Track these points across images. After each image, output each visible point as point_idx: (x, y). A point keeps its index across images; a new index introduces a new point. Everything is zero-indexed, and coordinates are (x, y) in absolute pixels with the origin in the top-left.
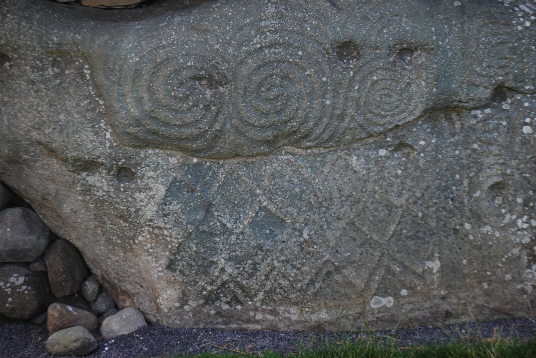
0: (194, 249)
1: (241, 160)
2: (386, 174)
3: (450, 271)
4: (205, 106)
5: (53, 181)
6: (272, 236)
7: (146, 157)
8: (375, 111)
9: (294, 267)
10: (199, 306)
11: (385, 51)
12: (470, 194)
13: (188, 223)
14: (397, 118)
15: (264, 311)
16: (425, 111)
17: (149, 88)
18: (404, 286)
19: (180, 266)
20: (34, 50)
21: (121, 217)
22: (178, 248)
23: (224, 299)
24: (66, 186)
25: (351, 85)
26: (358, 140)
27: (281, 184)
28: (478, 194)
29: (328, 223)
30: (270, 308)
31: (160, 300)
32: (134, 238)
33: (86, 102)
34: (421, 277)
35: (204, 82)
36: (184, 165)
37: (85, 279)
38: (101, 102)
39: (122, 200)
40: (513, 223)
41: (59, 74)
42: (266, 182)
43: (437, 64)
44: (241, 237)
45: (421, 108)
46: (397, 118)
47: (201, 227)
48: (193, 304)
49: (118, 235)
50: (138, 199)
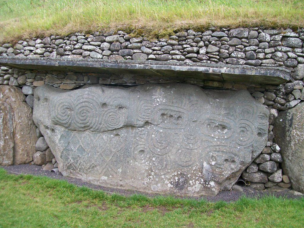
3: (124, 173)
6: (82, 154)
25: (103, 115)
34: (116, 173)
35: (69, 110)
42: (82, 139)
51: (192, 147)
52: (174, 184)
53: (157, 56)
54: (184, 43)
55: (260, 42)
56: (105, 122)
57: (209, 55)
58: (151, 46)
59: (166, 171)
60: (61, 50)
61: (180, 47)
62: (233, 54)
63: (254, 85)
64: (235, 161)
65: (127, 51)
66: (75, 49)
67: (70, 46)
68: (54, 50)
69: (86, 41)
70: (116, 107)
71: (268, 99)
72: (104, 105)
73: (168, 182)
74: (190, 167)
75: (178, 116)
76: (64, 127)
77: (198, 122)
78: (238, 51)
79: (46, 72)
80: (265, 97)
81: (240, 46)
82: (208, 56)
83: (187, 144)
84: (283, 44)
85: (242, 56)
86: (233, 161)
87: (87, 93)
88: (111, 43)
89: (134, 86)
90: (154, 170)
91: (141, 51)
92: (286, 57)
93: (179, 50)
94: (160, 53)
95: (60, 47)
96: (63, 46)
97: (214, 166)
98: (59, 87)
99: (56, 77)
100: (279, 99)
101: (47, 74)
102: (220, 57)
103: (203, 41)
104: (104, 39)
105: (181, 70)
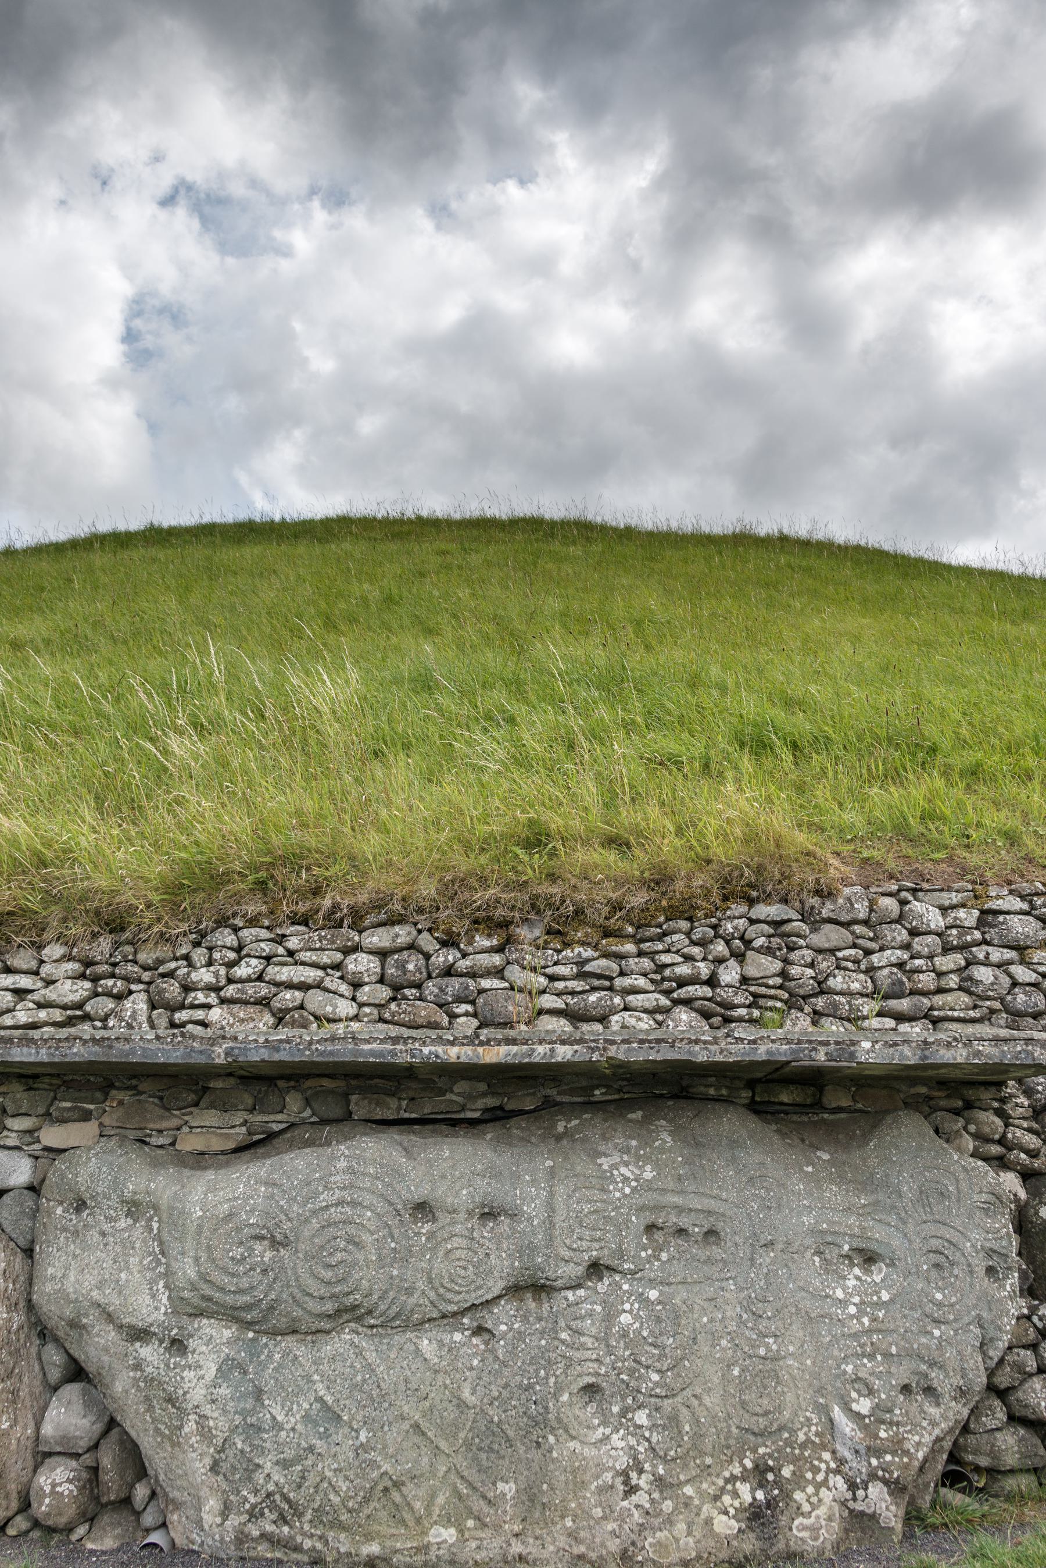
0: (240, 1446)
1: (299, 1336)
6: (326, 1436)
9: (346, 1478)
11: (462, 1216)
12: (556, 1396)
13: (236, 1413)
14: (473, 1295)
15: (312, 1536)
18: (470, 1514)
19: (225, 1466)
20: (109, 1199)
21: (170, 1400)
26: (429, 1320)
28: (565, 1397)
29: (390, 1424)
30: (319, 1533)
32: (180, 1428)
35: (266, 1242)
36: (238, 1339)
38: (163, 1260)
46: (473, 1295)
51: (774, 1347)
53: (569, 999)
55: (914, 933)
56: (430, 1280)
57: (752, 989)
60: (172, 989)
61: (646, 963)
62: (831, 982)
63: (923, 1090)
64: (935, 1389)
65: (454, 985)
66: (230, 981)
67: (212, 969)
68: (133, 987)
69: (281, 950)
70: (470, 1213)
71: (981, 1137)
72: (423, 1209)
74: (786, 1435)
75: (705, 1230)
76: (237, 1320)
78: (846, 969)
80: (972, 1128)
81: (852, 952)
82: (751, 994)
84: (987, 937)
86: (929, 1391)
87: (342, 1164)
88: (383, 954)
89: (497, 1116)
91: (507, 985)
92: (1006, 982)
93: (645, 975)
94: (579, 989)
95: (163, 975)
96: (176, 969)
97: (869, 1417)
98: (173, 1144)
99: (156, 1101)
100: (1019, 1133)
101: (114, 1092)
102: (791, 995)
103: (723, 938)
104: (357, 938)
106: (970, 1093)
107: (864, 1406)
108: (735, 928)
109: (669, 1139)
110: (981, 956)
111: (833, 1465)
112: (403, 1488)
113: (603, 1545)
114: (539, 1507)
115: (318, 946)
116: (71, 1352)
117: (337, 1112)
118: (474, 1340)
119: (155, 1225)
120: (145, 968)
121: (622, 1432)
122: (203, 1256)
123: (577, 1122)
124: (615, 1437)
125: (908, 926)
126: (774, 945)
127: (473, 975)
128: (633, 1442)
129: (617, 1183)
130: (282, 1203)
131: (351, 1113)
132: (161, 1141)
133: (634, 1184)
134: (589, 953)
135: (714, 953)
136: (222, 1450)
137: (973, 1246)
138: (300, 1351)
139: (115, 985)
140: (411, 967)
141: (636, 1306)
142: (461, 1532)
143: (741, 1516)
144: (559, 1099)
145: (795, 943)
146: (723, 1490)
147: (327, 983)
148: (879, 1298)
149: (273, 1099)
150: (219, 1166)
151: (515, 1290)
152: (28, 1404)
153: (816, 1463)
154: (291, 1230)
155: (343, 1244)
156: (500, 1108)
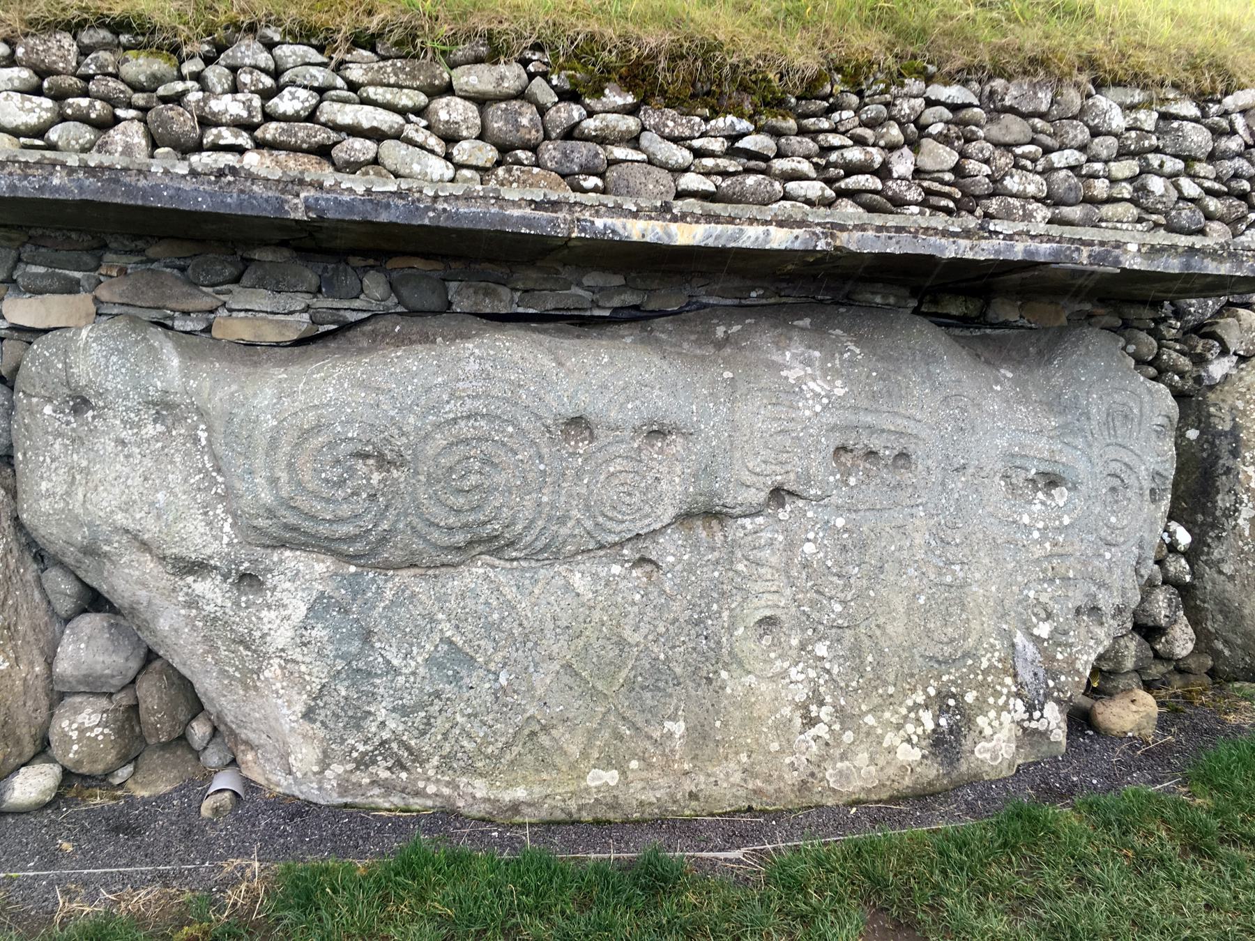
0: (343, 693)
1: (418, 571)
2: (620, 599)
3: (700, 736)
4: (369, 496)
5: (144, 585)
7: (281, 561)
8: (610, 514)
10: (346, 771)
11: (628, 433)
12: (731, 629)
13: (336, 657)
14: (639, 524)
16: (677, 517)
17: (290, 466)
18: (634, 755)
19: (321, 714)
20: (126, 398)
21: (241, 642)
22: (321, 690)
23: (383, 764)
24: (163, 594)
26: (583, 551)
27: (474, 607)
29: (536, 665)
30: (447, 778)
31: (291, 760)
32: (259, 671)
33: (197, 478)
35: (371, 461)
37: (194, 717)
38: (220, 479)
39: (242, 620)
40: (784, 674)
41: (164, 434)
42: (452, 604)
43: (696, 454)
44: (412, 679)
45: (671, 512)
47: (354, 663)
48: (338, 769)
49: (234, 665)
50: (265, 620)
51: (961, 574)
52: (924, 743)
54: (825, 124)
55: (1095, 133)
56: (588, 508)
57: (925, 184)
58: (687, 133)
59: (880, 691)
60: (182, 122)
61: (809, 144)
62: (1008, 182)
63: (1087, 307)
65: (582, 152)
66: (268, 117)
67: (239, 96)
71: (1140, 362)
72: (578, 424)
73: (897, 741)
74: (970, 662)
77: (971, 470)
78: (1024, 168)
79: (95, 244)
80: (1131, 348)
81: (1032, 148)
83: (941, 564)
85: (1040, 191)
86: (1095, 610)
87: (473, 366)
88: (481, 101)
89: (634, 317)
90: (828, 699)
91: (645, 157)
93: (808, 157)
94: (731, 169)
95: (165, 100)
96: (184, 93)
97: (1047, 640)
98: (208, 330)
101: (109, 257)
102: (964, 194)
104: (446, 76)
105: (969, 255)
106: (1132, 312)
107: (1044, 630)
108: (912, 109)
109: (858, 351)
110: (1156, 164)
111: (1014, 689)
112: (554, 732)
113: (781, 778)
114: (712, 745)
115: (392, 81)
116: (88, 581)
117: (433, 301)
118: (634, 573)
119: (203, 435)
120: (136, 88)
121: (801, 665)
122: (284, 477)
123: (739, 327)
124: (793, 671)
125: (1091, 124)
126: (953, 133)
127: (602, 140)
128: (812, 674)
129: (807, 399)
130: (392, 413)
131: (450, 304)
132: (190, 326)
133: (825, 401)
134: (744, 125)
135: (888, 138)
136: (320, 695)
137: (1147, 469)
138: (420, 587)
139: (91, 106)
140: (525, 121)
141: (821, 534)
142: (623, 773)
143: (924, 743)
144: (705, 300)
145: (973, 132)
146: (906, 717)
147: (409, 131)
148: (1061, 522)
149: (350, 280)
150: (285, 363)
151: (685, 518)
152: (31, 637)
153: (998, 688)
154: (408, 446)
155: (477, 465)
156: (636, 307)
